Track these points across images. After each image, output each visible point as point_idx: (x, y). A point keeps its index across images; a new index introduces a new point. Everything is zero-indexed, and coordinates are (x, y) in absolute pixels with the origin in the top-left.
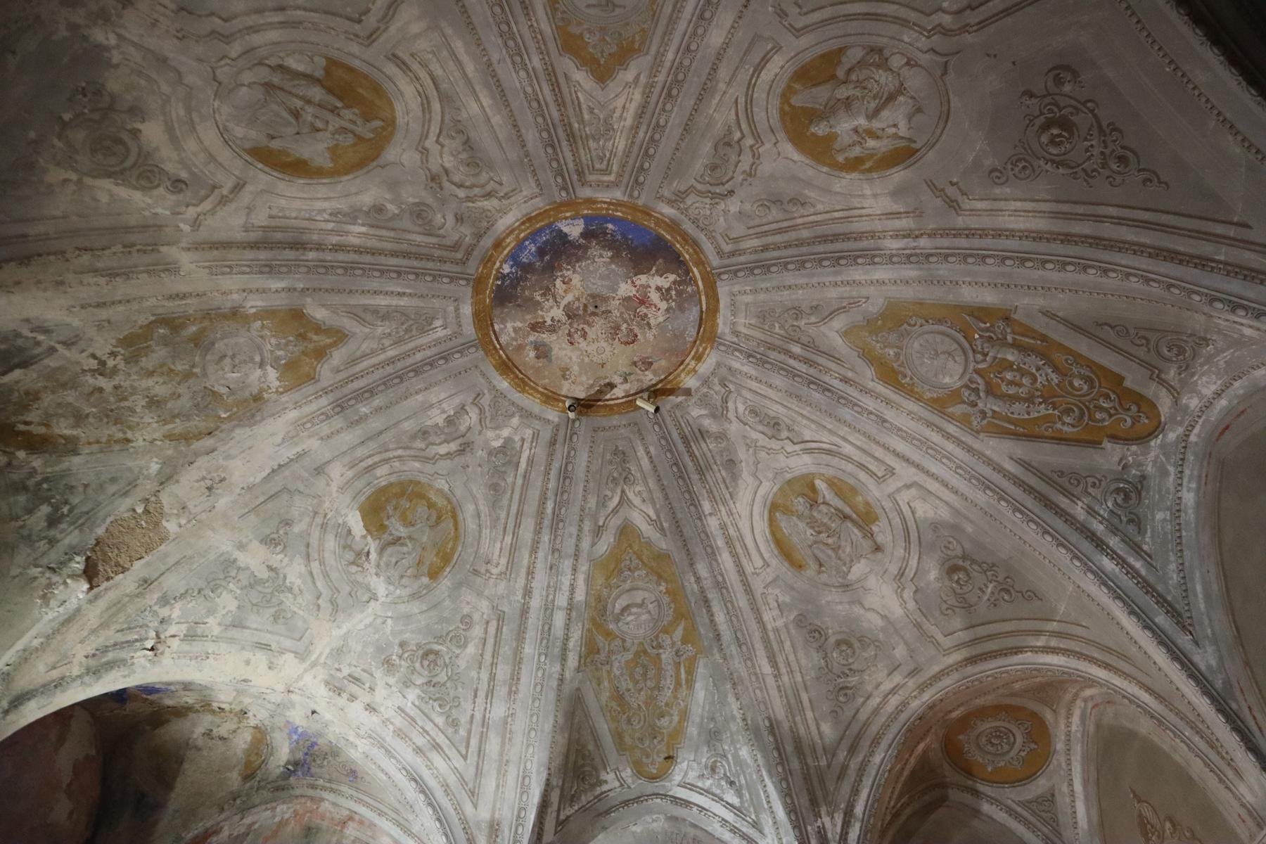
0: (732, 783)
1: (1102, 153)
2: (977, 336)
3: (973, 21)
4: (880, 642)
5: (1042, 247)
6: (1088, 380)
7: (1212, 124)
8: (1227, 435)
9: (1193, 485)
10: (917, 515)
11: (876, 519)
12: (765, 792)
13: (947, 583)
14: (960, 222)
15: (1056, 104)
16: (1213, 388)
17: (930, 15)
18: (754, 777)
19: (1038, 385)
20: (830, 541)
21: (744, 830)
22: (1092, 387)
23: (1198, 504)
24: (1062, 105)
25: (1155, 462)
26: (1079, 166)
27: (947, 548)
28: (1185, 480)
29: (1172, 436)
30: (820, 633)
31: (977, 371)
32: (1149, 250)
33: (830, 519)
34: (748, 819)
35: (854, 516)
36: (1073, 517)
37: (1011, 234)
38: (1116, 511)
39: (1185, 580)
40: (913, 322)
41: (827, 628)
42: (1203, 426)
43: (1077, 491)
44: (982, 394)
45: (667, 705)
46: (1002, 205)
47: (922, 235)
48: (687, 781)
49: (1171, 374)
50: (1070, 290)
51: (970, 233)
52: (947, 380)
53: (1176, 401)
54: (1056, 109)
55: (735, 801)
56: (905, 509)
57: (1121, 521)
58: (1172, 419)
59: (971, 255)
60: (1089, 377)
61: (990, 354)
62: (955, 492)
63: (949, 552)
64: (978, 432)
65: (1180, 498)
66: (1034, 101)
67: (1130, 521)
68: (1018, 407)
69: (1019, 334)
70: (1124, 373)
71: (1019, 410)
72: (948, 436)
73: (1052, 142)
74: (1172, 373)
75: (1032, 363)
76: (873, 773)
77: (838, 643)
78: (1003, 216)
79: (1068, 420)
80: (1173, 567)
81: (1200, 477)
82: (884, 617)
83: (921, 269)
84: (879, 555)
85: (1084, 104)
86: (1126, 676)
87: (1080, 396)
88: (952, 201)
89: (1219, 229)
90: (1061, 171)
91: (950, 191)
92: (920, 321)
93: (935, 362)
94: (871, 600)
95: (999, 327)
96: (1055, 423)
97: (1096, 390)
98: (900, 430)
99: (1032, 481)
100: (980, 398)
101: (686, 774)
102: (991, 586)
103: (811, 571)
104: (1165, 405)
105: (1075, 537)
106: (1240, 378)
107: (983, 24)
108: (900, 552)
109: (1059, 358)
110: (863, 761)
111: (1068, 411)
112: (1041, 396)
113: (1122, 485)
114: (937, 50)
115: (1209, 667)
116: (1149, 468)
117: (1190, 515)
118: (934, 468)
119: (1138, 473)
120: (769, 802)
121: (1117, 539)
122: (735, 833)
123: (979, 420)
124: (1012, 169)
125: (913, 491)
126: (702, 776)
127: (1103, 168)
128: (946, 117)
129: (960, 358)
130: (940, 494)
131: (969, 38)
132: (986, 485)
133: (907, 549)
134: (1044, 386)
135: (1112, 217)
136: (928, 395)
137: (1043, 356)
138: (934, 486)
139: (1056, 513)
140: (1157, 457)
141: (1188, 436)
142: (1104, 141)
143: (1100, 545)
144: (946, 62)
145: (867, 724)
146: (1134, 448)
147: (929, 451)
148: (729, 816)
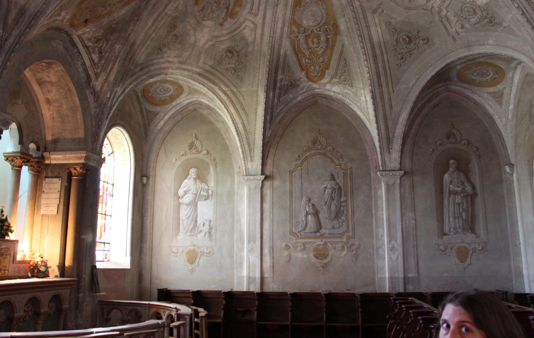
0: (100, 53)
1: (403, 53)
2: (326, 27)
3: (443, 20)
4: (185, 46)
5: (368, 41)
6: (323, 61)
7: (417, 77)
8: (324, 100)
9: (303, 97)
10: (243, 31)
11: (233, 18)
12: (112, 67)
13: (224, 52)
14: (369, 14)
15: (416, 39)
16: (336, 90)
17: (446, 8)
18: (113, 58)
19: (315, 49)
20: (214, 8)
21: (90, 73)
22: (321, 63)
23: (299, 102)
24: (416, 41)
25: (304, 85)
26: (398, 47)
27: (237, 46)
28: (303, 95)
29: (315, 86)
30: (174, 27)
31: (312, 31)
33: (224, 3)
34: (96, 70)
35: (230, 11)
36: (277, 77)
37: (369, 31)
39: (279, 113)
40: (323, 5)
41: (178, 28)
42: (321, 91)
43: (285, 73)
44: (304, 34)
45: (109, 4)
46: (378, 26)
47: (360, 2)
48: (82, 37)
49: (335, 80)
50: (355, 51)
51: (365, 18)
52: (305, 22)
53: (327, 83)
54: (414, 39)
55: (96, 60)
56: (244, 25)
57: (284, 89)
58: (321, 84)
59: (357, 20)
60: (325, 61)
61: (321, 33)
62: (262, 39)
63: (236, 47)
64: (289, 38)
65: (298, 97)
66: (416, 33)
67: (285, 91)
68: (305, 46)
69: (332, 40)
70: (330, 68)
71: (303, 47)
72: (282, 29)
73: (403, 39)
74: (336, 80)
75: (324, 45)
77: (175, 35)
78: (375, 28)
79: (307, 60)
80: (280, 108)
81: (307, 97)
82: (195, 41)
83: (346, 4)
84: (219, 27)
85: (417, 46)
86: (241, 118)
87: (317, 61)
88: (376, 11)
89: (390, 86)
90: (395, 43)
91: (380, 10)
92: (325, 7)
93: (310, 16)
94: (199, 35)
95: (332, 33)
96: (304, 58)
97: (320, 64)
98: (276, 12)
99: (281, 60)
100: (303, 34)
101: (84, 34)
102: (233, 65)
103: (196, 8)
104: (323, 81)
105: (272, 82)
106: (343, 96)
107: (442, 22)
108: (225, 32)
109: (328, 52)
111: (310, 59)
112: (312, 51)
113: (293, 82)
114: (433, 8)
115: (267, 135)
118: (267, 29)
119: (299, 84)
120: (110, 71)
122: (85, 71)
123: (294, 36)
124: (392, 28)
125: (252, 25)
126: (89, 40)
127: (398, 53)
128: (408, 9)
129: (315, 23)
130: (257, 35)
131: (437, 18)
132: (272, 49)
133: (227, 34)
134: (316, 51)
135: (384, 59)
136: (295, 17)
137: (327, 47)
138: (259, 31)
139: (275, 72)
141: (316, 89)
142: (406, 53)
143: (274, 88)
144: (428, 10)
145: (153, 65)
146: (306, 79)
147: (273, 25)
148: (88, 63)
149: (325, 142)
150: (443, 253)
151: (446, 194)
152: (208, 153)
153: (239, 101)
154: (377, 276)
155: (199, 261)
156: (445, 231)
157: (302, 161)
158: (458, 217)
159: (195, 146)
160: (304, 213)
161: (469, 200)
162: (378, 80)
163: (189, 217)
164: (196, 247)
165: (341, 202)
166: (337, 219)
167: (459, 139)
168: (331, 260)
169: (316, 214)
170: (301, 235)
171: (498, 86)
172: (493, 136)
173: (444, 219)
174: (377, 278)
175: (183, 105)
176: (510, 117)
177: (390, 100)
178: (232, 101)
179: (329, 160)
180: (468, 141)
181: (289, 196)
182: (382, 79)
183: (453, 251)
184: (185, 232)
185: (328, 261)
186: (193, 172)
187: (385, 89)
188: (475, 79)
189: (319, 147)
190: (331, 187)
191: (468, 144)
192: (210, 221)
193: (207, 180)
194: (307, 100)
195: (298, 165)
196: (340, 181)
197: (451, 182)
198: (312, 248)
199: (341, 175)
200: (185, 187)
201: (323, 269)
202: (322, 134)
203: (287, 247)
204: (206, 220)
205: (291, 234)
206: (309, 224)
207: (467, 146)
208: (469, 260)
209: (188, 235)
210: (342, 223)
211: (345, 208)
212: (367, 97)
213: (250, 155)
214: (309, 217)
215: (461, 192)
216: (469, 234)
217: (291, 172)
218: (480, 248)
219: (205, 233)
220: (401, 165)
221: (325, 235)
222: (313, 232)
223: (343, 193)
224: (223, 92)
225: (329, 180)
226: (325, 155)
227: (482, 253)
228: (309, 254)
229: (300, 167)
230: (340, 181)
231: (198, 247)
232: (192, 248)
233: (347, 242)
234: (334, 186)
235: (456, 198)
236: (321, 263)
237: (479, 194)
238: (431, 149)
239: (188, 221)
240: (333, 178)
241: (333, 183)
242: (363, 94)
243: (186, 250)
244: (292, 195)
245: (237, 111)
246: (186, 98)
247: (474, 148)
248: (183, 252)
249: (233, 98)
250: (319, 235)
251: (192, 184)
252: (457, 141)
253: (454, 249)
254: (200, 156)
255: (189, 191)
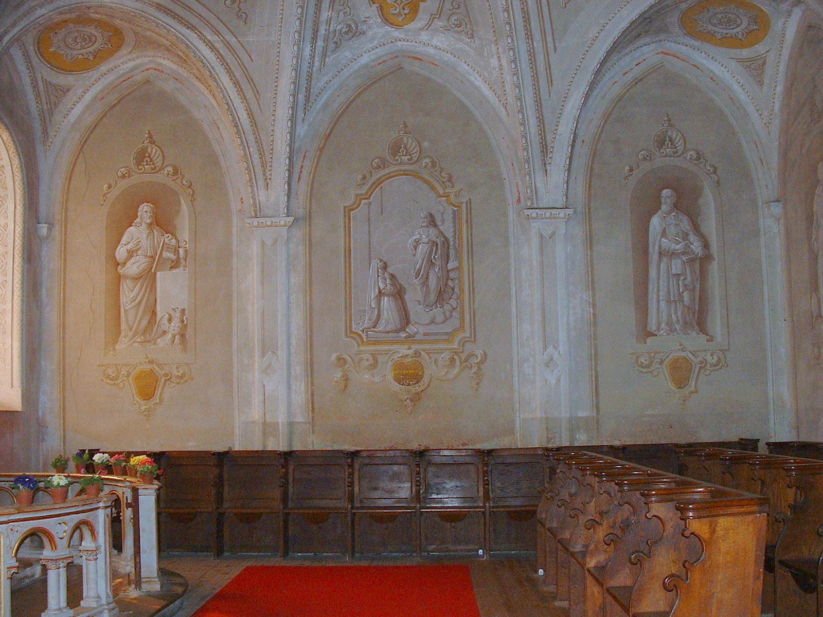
8: (417, 63)
9: (373, 57)
16: (439, 44)
23: (365, 66)
29: (396, 34)
32: (525, 7)
38: (337, 32)
43: (337, 7)
49: (438, 23)
67: (336, 43)
76: (32, 19)
80: (326, 78)
81: (380, 58)
86: (244, 98)
89: (549, 39)
105: (310, 24)
110: (34, 7)
115: (299, 135)
116: (370, 33)
117: (356, 66)
121: (323, 44)
140: (379, 33)
143: (314, 39)
146: (379, 20)
149: (417, 149)
150: (645, 370)
151: (654, 256)
152: (176, 172)
153: (242, 65)
154: (519, 417)
155: (161, 395)
156: (651, 329)
157: (370, 188)
158: (675, 302)
159: (149, 157)
160: (374, 292)
161: (697, 266)
162: (525, 26)
163: (140, 302)
164: (155, 366)
165: (448, 271)
166: (440, 304)
167: (680, 148)
168: (429, 385)
169: (399, 294)
170: (367, 335)
171: (756, 46)
172: (744, 145)
173: (649, 305)
174: (518, 419)
175: (122, 72)
176: (776, 109)
177: (548, 66)
178: (227, 64)
179: (425, 186)
180: (698, 153)
181: (343, 259)
182: (532, 24)
183: (664, 367)
184: (131, 334)
185: (422, 388)
186: (145, 211)
187: (538, 45)
188: (715, 32)
189: (405, 158)
190: (430, 240)
191: (698, 158)
192: (183, 311)
193: (175, 227)
194: (380, 64)
195: (362, 195)
196: (448, 229)
197: (664, 234)
198: (390, 363)
199: (449, 216)
200: (129, 243)
201: (412, 404)
202: (410, 133)
203: (341, 361)
204: (174, 310)
205: (348, 335)
206: (385, 315)
207: (696, 162)
208: (693, 383)
209: (139, 340)
210: (451, 312)
211: (457, 282)
212: (502, 59)
213: (264, 175)
214: (385, 301)
215: (683, 253)
216: (694, 334)
217: (347, 209)
218: (714, 361)
219: (174, 336)
220: (567, 198)
221: (417, 337)
222: (392, 332)
223: (452, 252)
224: (207, 45)
225: (424, 227)
226: (416, 175)
227: (717, 370)
228: (385, 375)
229: (365, 199)
230: (448, 229)
231: (159, 365)
232: (148, 367)
233: (461, 351)
234: (434, 239)
235: (673, 263)
236: (409, 391)
237: (715, 256)
238: (627, 168)
239: (137, 314)
240: (432, 221)
241: (432, 231)
242: (494, 52)
243: (134, 373)
244: (350, 257)
245: (237, 84)
246: (129, 57)
247: (709, 168)
248: (128, 376)
249: (229, 58)
250: (405, 338)
251: (145, 236)
252: (677, 152)
253: (665, 363)
254: (159, 178)
255: (138, 250)
